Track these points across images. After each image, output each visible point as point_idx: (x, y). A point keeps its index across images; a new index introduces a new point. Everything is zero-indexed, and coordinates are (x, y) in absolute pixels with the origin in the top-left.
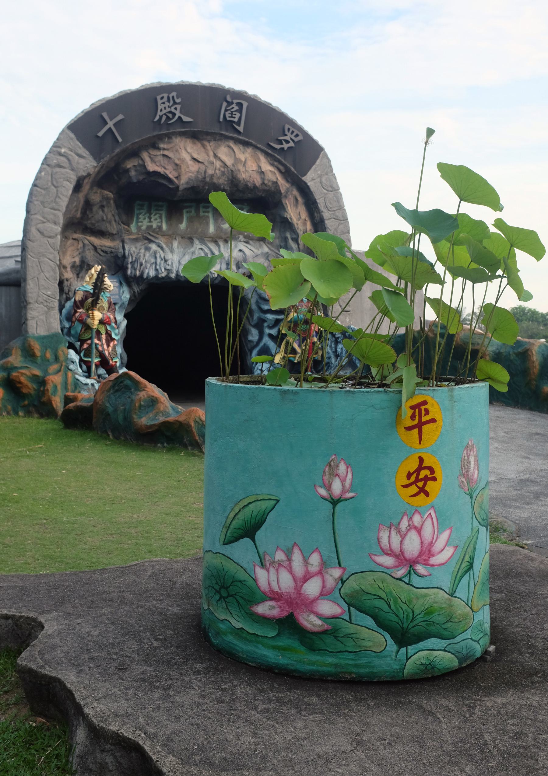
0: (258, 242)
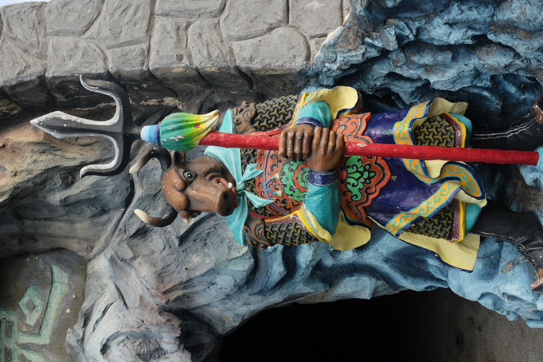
0: (91, 282)
